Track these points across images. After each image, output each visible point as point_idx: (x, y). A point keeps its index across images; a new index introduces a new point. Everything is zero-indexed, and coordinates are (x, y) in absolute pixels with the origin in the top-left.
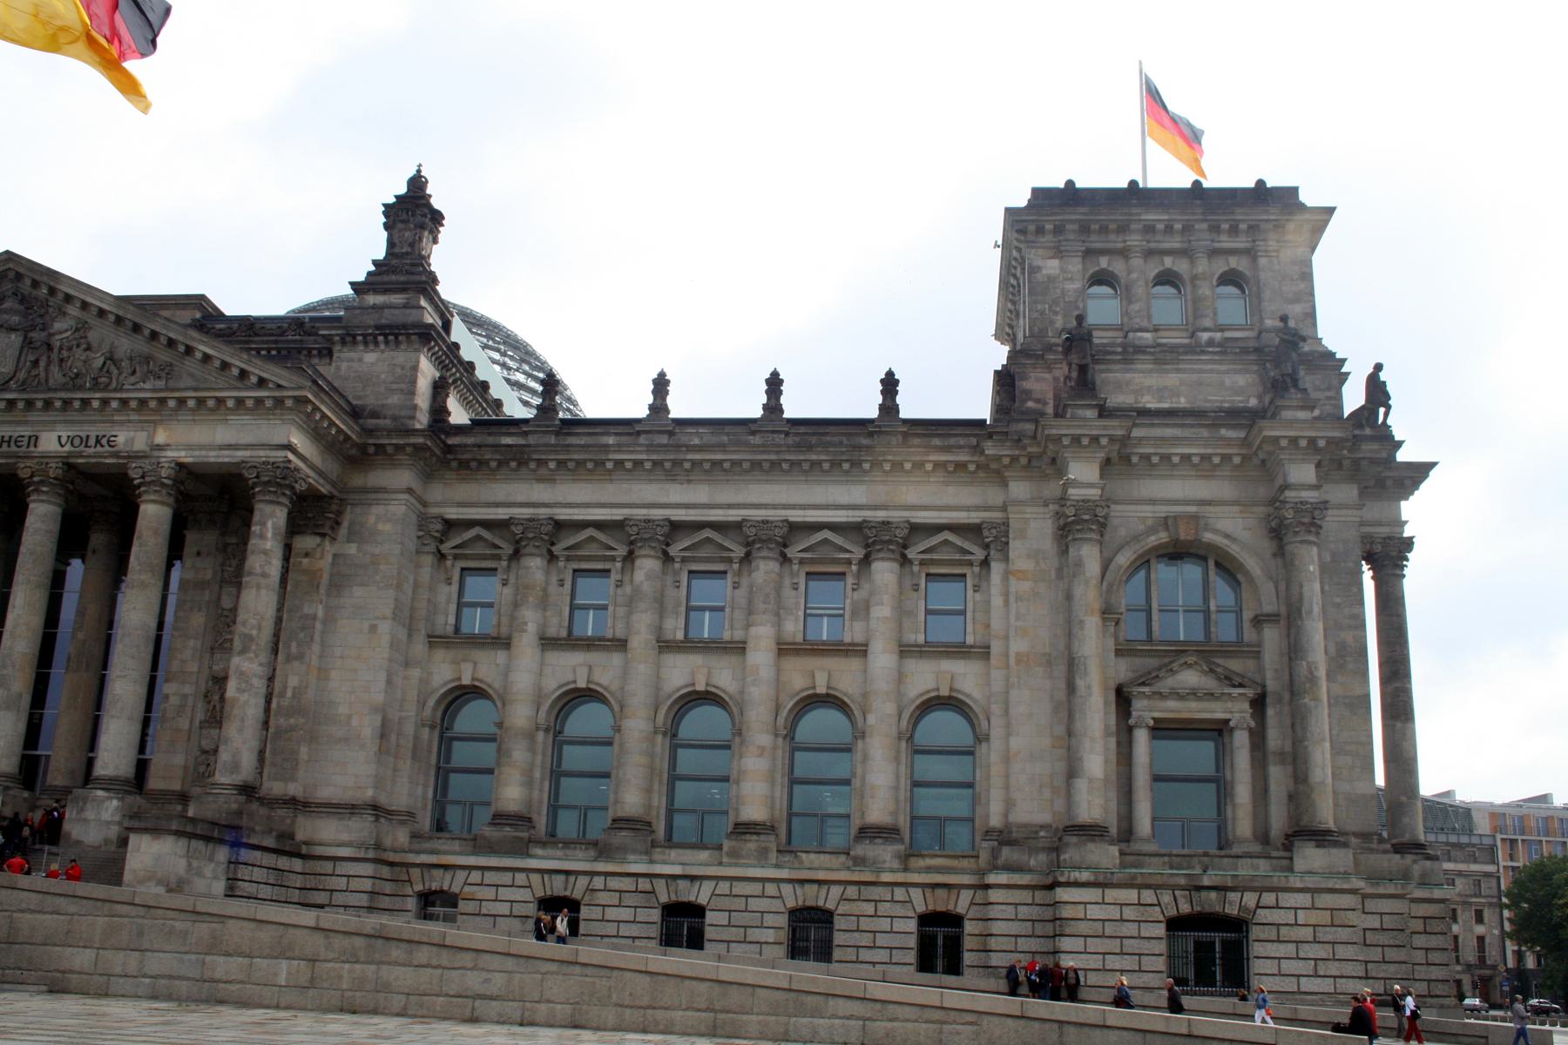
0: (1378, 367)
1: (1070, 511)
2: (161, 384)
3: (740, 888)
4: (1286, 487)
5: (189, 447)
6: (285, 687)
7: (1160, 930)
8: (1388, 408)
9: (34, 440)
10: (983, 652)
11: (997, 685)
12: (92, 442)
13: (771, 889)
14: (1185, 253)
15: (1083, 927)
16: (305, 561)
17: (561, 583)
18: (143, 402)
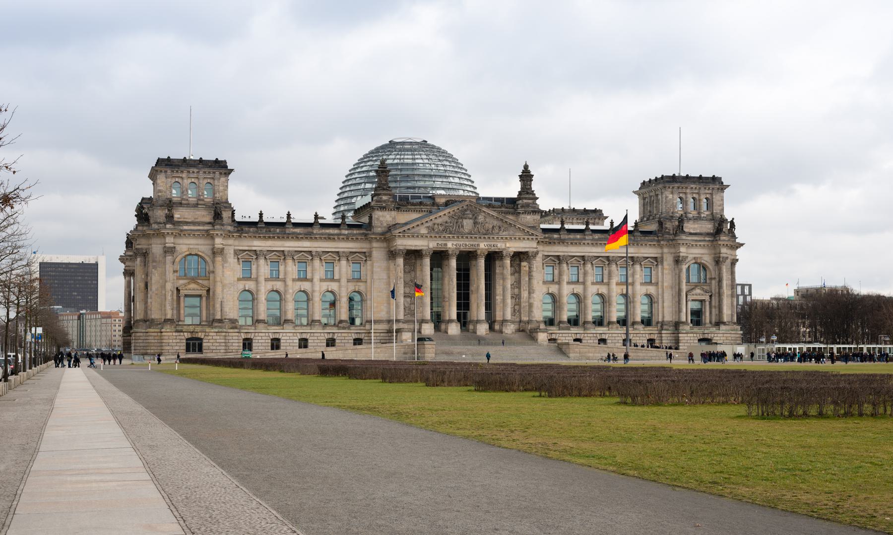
0: (733, 219)
1: (681, 258)
2: (507, 232)
3: (614, 335)
4: (720, 253)
5: (515, 248)
6: (524, 297)
7: (697, 341)
8: (735, 229)
9: (478, 245)
10: (657, 284)
11: (660, 292)
12: (492, 246)
13: (620, 335)
14: (698, 194)
15: (684, 341)
16: (525, 268)
17: (568, 269)
18: (506, 238)
